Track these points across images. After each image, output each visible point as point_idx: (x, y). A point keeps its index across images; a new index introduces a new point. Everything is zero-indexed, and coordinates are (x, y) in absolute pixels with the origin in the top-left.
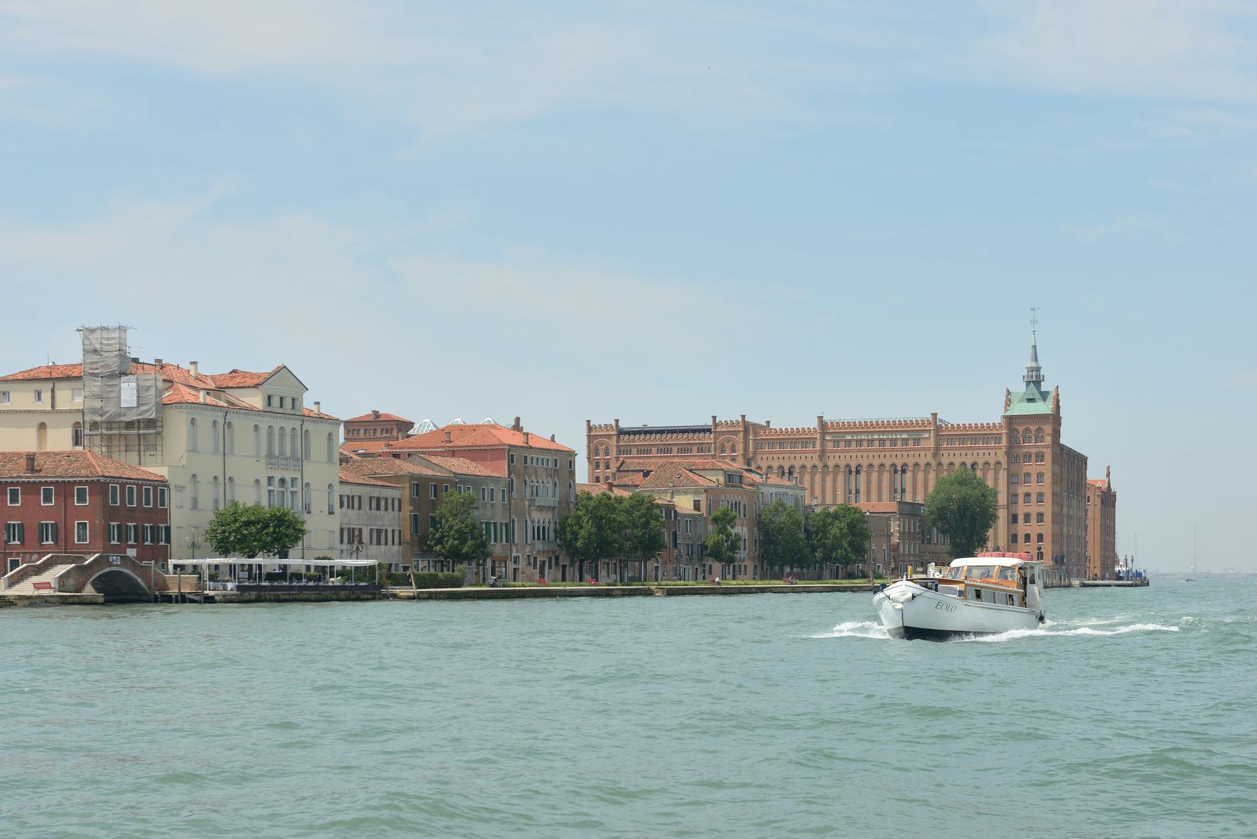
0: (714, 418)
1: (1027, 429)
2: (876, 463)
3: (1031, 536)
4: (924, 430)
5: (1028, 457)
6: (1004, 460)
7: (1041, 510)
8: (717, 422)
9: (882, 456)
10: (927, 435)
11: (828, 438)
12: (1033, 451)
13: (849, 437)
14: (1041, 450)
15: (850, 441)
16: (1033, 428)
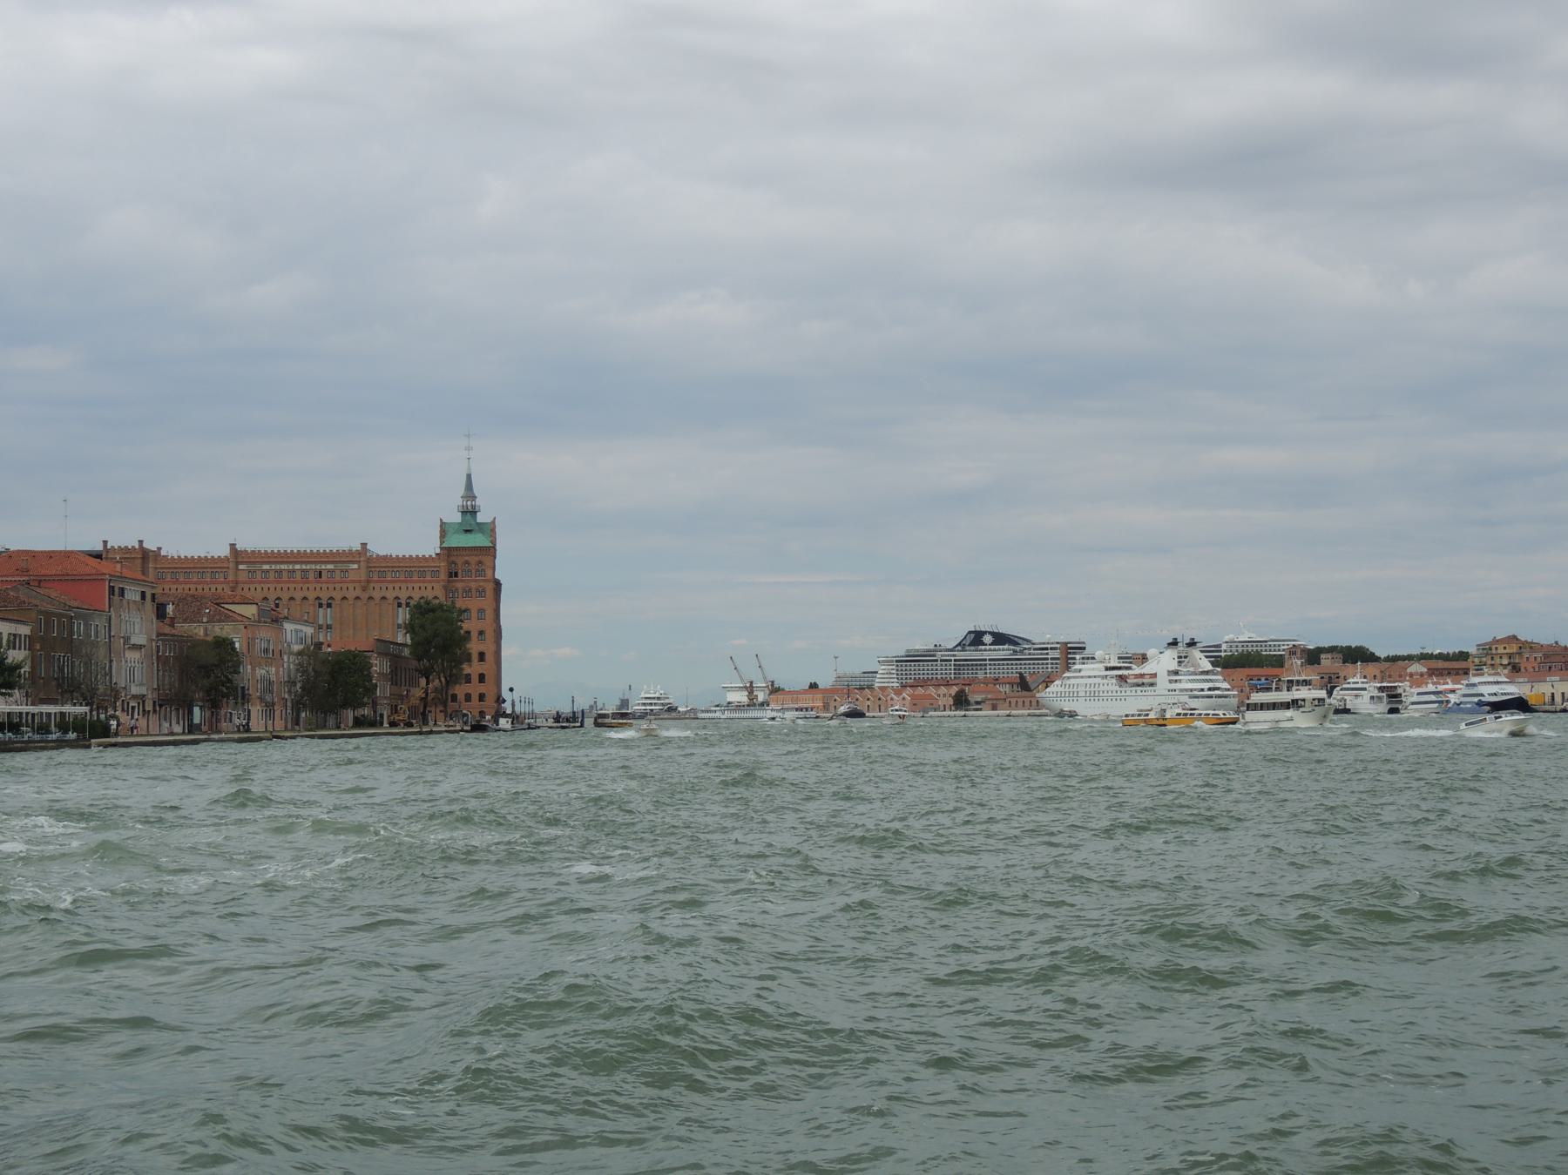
0: (105, 543)
1: (467, 562)
2: (298, 595)
5: (468, 592)
8: (109, 547)
9: (305, 588)
10: (356, 566)
11: (241, 567)
13: (266, 567)
15: (268, 571)
16: (473, 560)
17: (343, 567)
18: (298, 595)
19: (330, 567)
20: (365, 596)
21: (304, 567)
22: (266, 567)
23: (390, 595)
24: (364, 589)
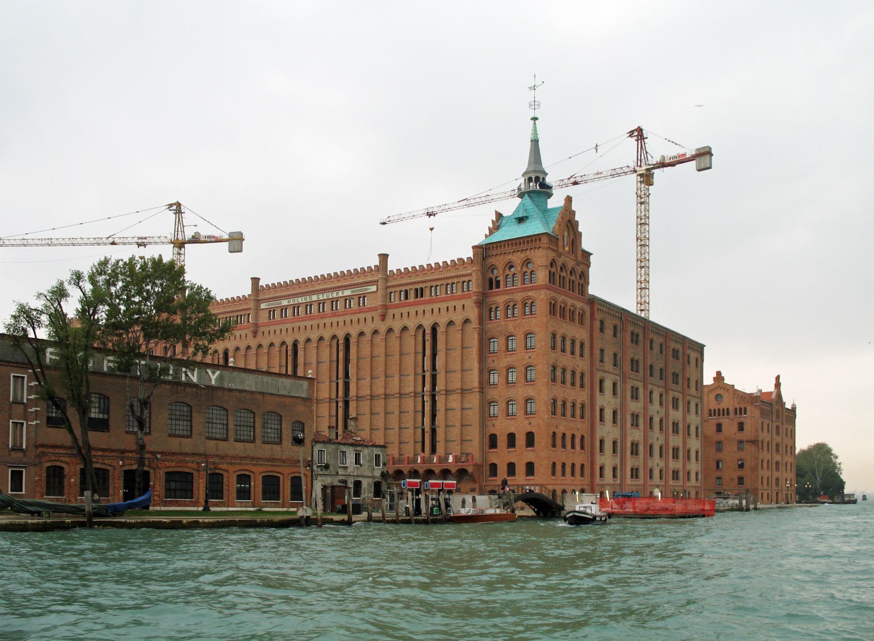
3: (517, 436)
4: (370, 282)
6: (473, 313)
7: (530, 392)
10: (373, 288)
11: (263, 306)
12: (519, 297)
13: (285, 303)
14: (530, 294)
16: (517, 258)
17: (359, 291)
18: (314, 336)
19: (348, 293)
20: (383, 328)
21: (321, 297)
22: (285, 303)
23: (412, 324)
24: (383, 317)
